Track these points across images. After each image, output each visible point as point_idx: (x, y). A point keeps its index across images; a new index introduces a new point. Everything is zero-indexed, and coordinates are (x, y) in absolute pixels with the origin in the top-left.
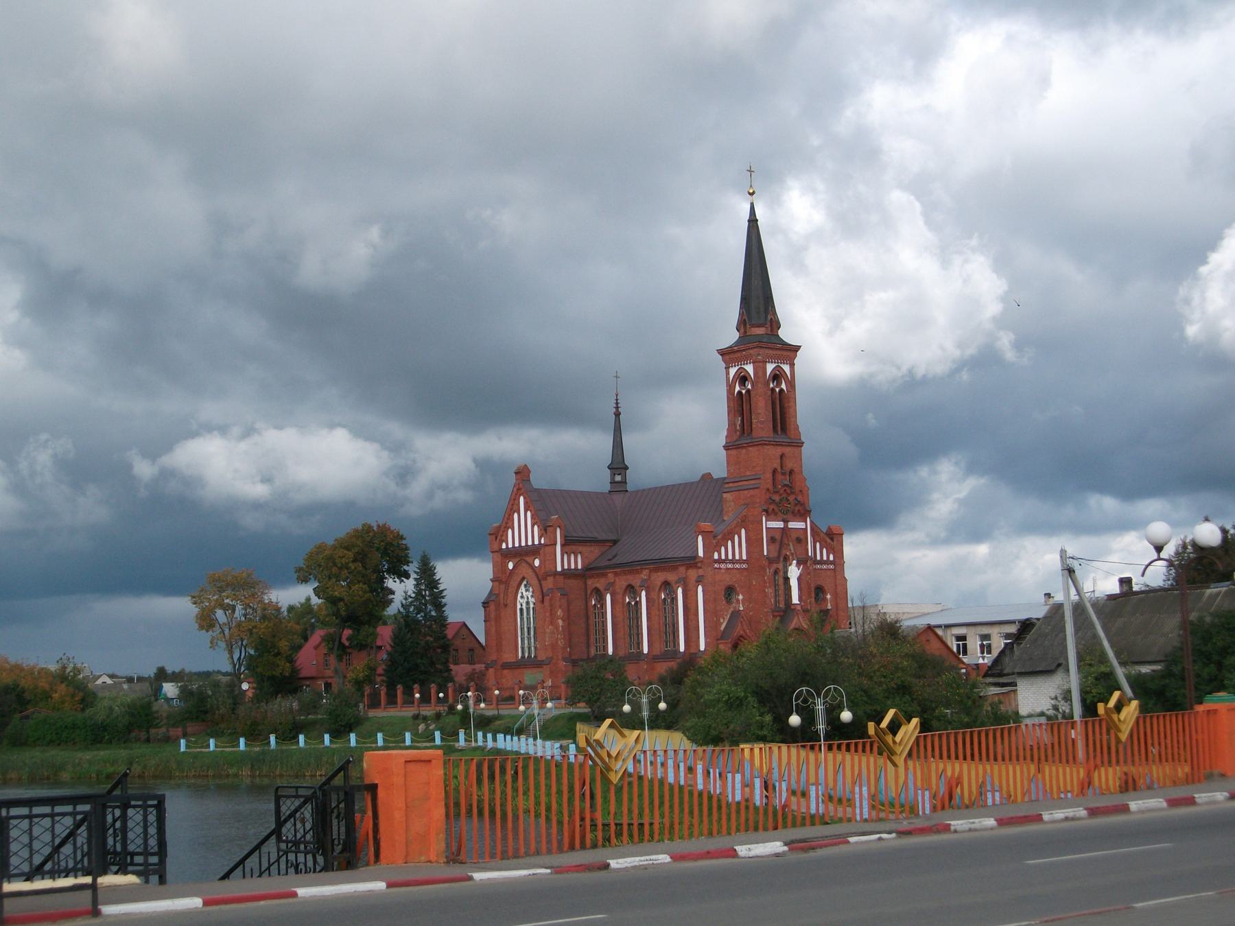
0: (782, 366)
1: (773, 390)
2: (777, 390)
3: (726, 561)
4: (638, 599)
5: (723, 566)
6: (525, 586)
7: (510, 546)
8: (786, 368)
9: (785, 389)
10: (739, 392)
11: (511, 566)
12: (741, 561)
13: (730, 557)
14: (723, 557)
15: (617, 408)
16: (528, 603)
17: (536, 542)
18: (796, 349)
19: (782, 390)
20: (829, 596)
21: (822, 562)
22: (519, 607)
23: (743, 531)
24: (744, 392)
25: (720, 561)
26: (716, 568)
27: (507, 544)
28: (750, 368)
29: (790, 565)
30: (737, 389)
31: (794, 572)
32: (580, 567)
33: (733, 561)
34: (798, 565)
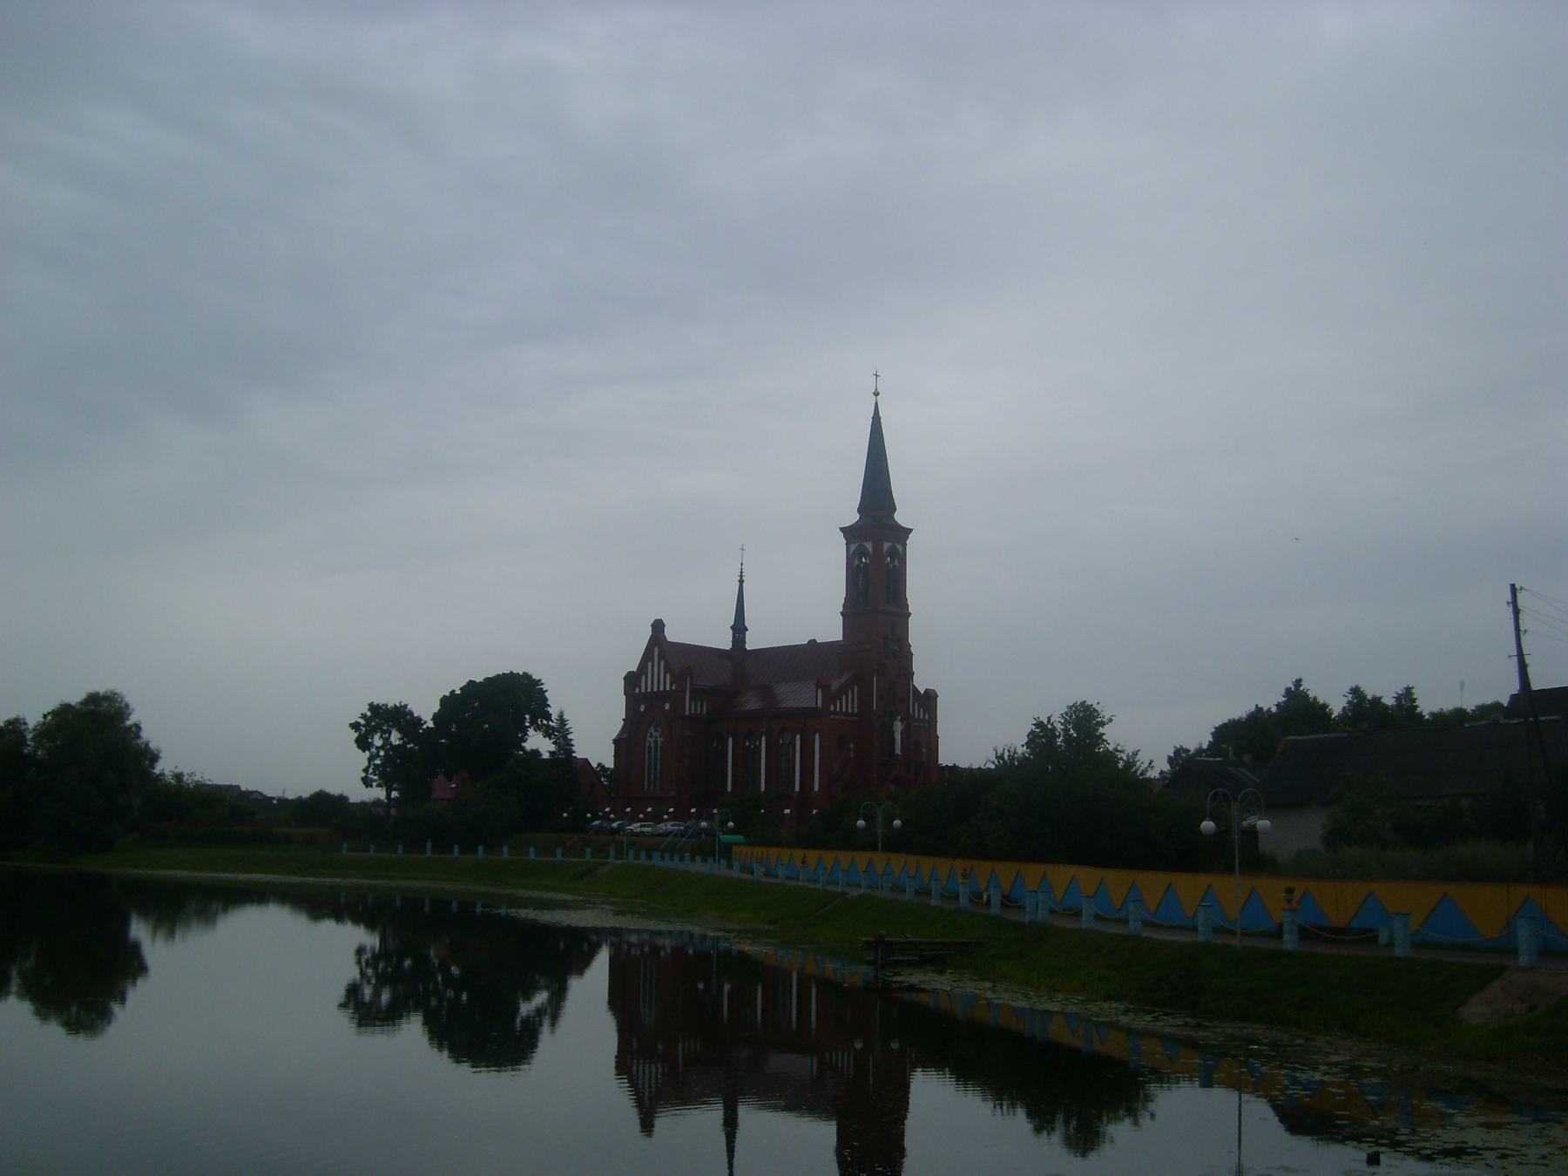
4: (757, 743)
5: (837, 717)
6: (655, 727)
7: (643, 690)
8: (899, 547)
10: (858, 565)
11: (642, 708)
12: (852, 714)
13: (844, 710)
14: (838, 710)
15: (741, 576)
16: (656, 742)
17: (668, 688)
19: (895, 566)
20: (924, 750)
21: (918, 720)
22: (648, 745)
23: (856, 688)
25: (835, 713)
27: (640, 690)
28: (869, 545)
29: (895, 720)
30: (856, 562)
31: (898, 726)
32: (704, 712)
33: (847, 714)
34: (901, 721)
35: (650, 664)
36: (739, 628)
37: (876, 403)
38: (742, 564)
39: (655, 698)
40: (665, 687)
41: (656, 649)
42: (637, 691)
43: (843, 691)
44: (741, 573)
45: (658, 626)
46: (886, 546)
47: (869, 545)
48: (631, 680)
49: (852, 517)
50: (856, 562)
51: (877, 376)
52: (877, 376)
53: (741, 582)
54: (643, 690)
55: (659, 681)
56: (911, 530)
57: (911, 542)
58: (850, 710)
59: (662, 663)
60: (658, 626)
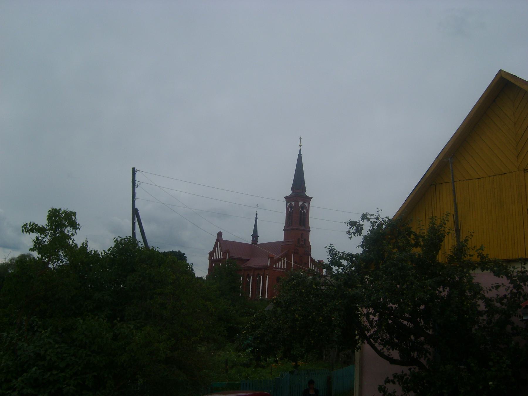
0: (305, 203)
1: (301, 211)
2: (302, 211)
3: (278, 268)
7: (214, 258)
8: (306, 204)
9: (305, 211)
10: (290, 211)
12: (284, 269)
13: (280, 267)
15: (256, 216)
17: (221, 258)
18: (311, 198)
19: (304, 212)
24: (291, 211)
25: (276, 268)
26: (274, 270)
27: (213, 258)
28: (293, 203)
30: (289, 210)
33: (281, 268)
35: (217, 248)
36: (255, 236)
37: (300, 149)
38: (257, 212)
39: (217, 261)
40: (220, 257)
41: (219, 243)
42: (212, 258)
43: (279, 260)
44: (257, 215)
45: (220, 234)
46: (300, 204)
47: (293, 203)
48: (211, 254)
49: (289, 192)
50: (289, 210)
51: (301, 139)
52: (301, 139)
53: (256, 218)
54: (214, 258)
55: (218, 255)
56: (312, 198)
57: (312, 203)
58: (280, 267)
59: (220, 248)
60: (220, 234)
